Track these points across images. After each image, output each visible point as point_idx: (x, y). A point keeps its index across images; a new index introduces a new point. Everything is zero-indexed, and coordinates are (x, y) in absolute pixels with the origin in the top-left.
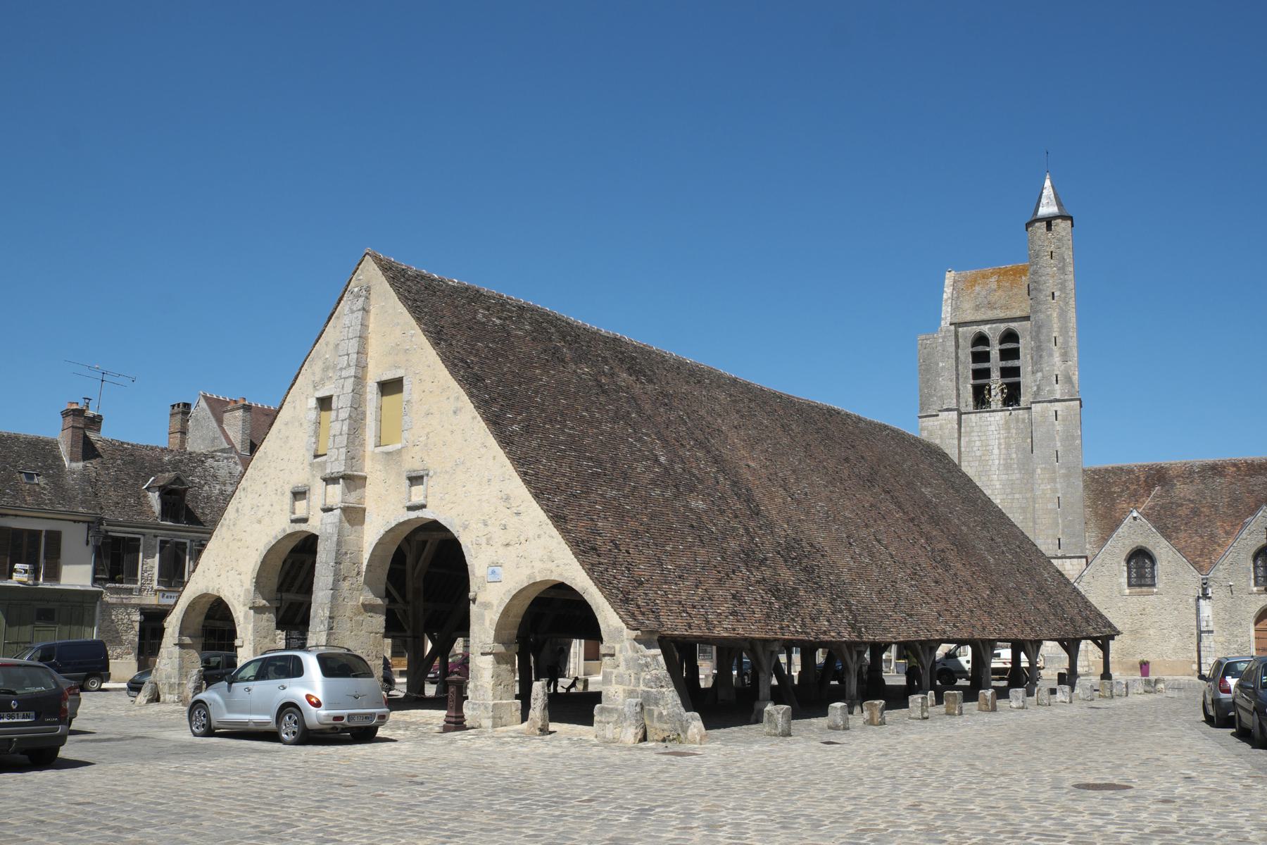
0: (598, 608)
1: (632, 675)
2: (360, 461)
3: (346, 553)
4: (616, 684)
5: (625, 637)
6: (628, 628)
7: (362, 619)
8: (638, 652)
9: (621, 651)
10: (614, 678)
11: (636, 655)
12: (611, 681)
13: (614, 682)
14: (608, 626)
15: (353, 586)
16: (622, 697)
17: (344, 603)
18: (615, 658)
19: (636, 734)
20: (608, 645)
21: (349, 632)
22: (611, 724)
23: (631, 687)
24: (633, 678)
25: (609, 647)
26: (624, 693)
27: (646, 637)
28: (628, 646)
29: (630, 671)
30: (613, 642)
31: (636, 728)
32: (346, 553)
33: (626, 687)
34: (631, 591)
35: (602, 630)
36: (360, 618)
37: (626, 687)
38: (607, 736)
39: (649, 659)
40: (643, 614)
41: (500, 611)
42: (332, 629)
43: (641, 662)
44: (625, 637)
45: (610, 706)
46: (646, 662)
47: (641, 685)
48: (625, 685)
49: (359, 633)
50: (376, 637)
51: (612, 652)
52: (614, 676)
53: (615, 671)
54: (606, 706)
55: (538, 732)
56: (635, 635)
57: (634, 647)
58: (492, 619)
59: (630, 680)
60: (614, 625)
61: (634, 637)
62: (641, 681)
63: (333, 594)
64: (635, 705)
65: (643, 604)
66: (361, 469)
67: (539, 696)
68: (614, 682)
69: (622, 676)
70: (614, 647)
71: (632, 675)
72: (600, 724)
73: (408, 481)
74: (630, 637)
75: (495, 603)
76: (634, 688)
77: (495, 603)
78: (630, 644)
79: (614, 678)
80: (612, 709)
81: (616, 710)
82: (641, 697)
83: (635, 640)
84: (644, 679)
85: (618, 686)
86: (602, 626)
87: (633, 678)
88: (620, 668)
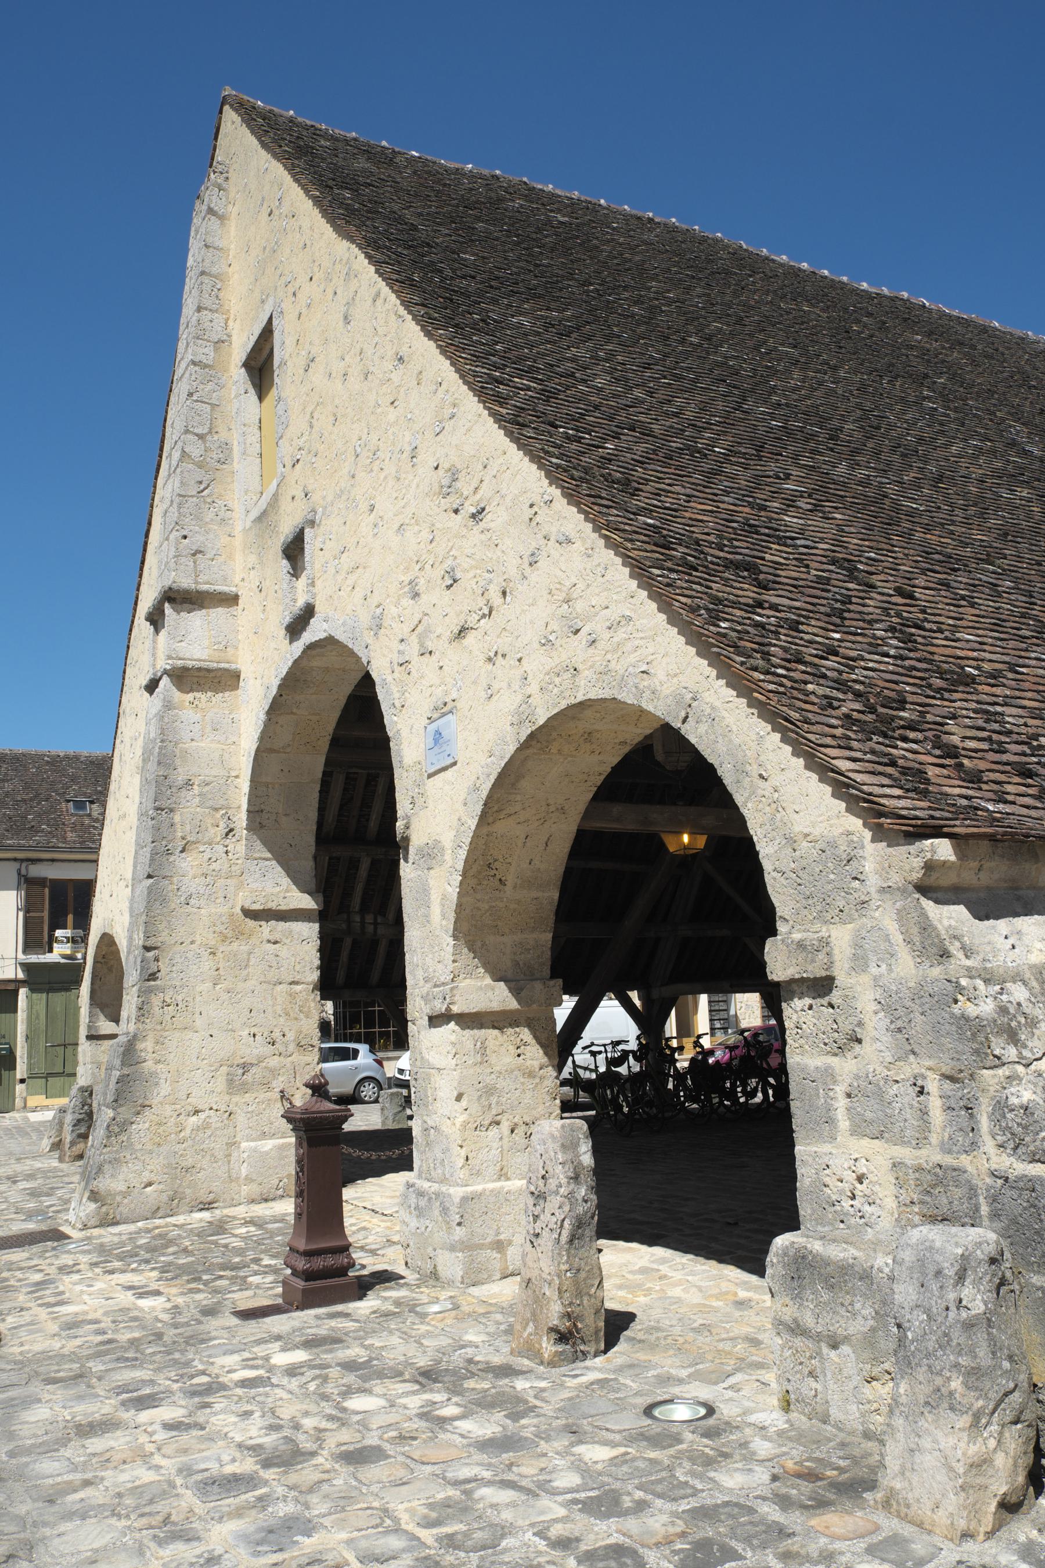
0: (741, 771)
1: (933, 1085)
2: (221, 559)
3: (188, 784)
4: (856, 1131)
5: (873, 882)
6: (880, 834)
7: (244, 948)
8: (945, 954)
9: (859, 962)
10: (841, 1103)
11: (936, 972)
12: (830, 1121)
13: (844, 1123)
14: (791, 841)
15: (214, 866)
16: (890, 1203)
17: (189, 909)
18: (835, 997)
19: (980, 1465)
20: (797, 936)
21: (209, 985)
22: (845, 1349)
23: (931, 1155)
24: (935, 1104)
25: (801, 945)
26: (900, 1183)
27: (985, 879)
28: (891, 926)
29: (909, 1068)
30: (819, 917)
31: (976, 1425)
32: (188, 784)
33: (905, 1154)
34: (910, 698)
35: (767, 865)
36: (240, 947)
37: (905, 1154)
38: (835, 1413)
39: (1019, 993)
40: (975, 778)
41: (460, 865)
42: (153, 977)
43: (972, 1010)
44: (873, 882)
45: (837, 1253)
46: (1003, 1010)
47: (989, 1145)
48: (903, 1142)
49: (241, 986)
50: (292, 996)
51: (816, 971)
52: (840, 1090)
53: (845, 1067)
54: (817, 1246)
55: (548, 1347)
56: (918, 863)
57: (926, 927)
58: (444, 897)
59: (924, 1112)
60: (816, 832)
61: (917, 876)
62: (984, 1123)
63: (150, 890)
64: (950, 1272)
65: (972, 744)
66: (225, 579)
67: (552, 1183)
68: (844, 1123)
69: (880, 1094)
70: (825, 943)
71: (933, 1085)
72: (799, 1342)
73: (285, 562)
74: (896, 879)
75: (447, 839)
76: (948, 1160)
77: (447, 839)
78: (901, 916)
79: (841, 1103)
80: (845, 1269)
81: (866, 1276)
82: (995, 1215)
83: (924, 889)
84: (1001, 1107)
85: (865, 1146)
86: (767, 851)
87: (935, 1104)
88: (867, 1049)
